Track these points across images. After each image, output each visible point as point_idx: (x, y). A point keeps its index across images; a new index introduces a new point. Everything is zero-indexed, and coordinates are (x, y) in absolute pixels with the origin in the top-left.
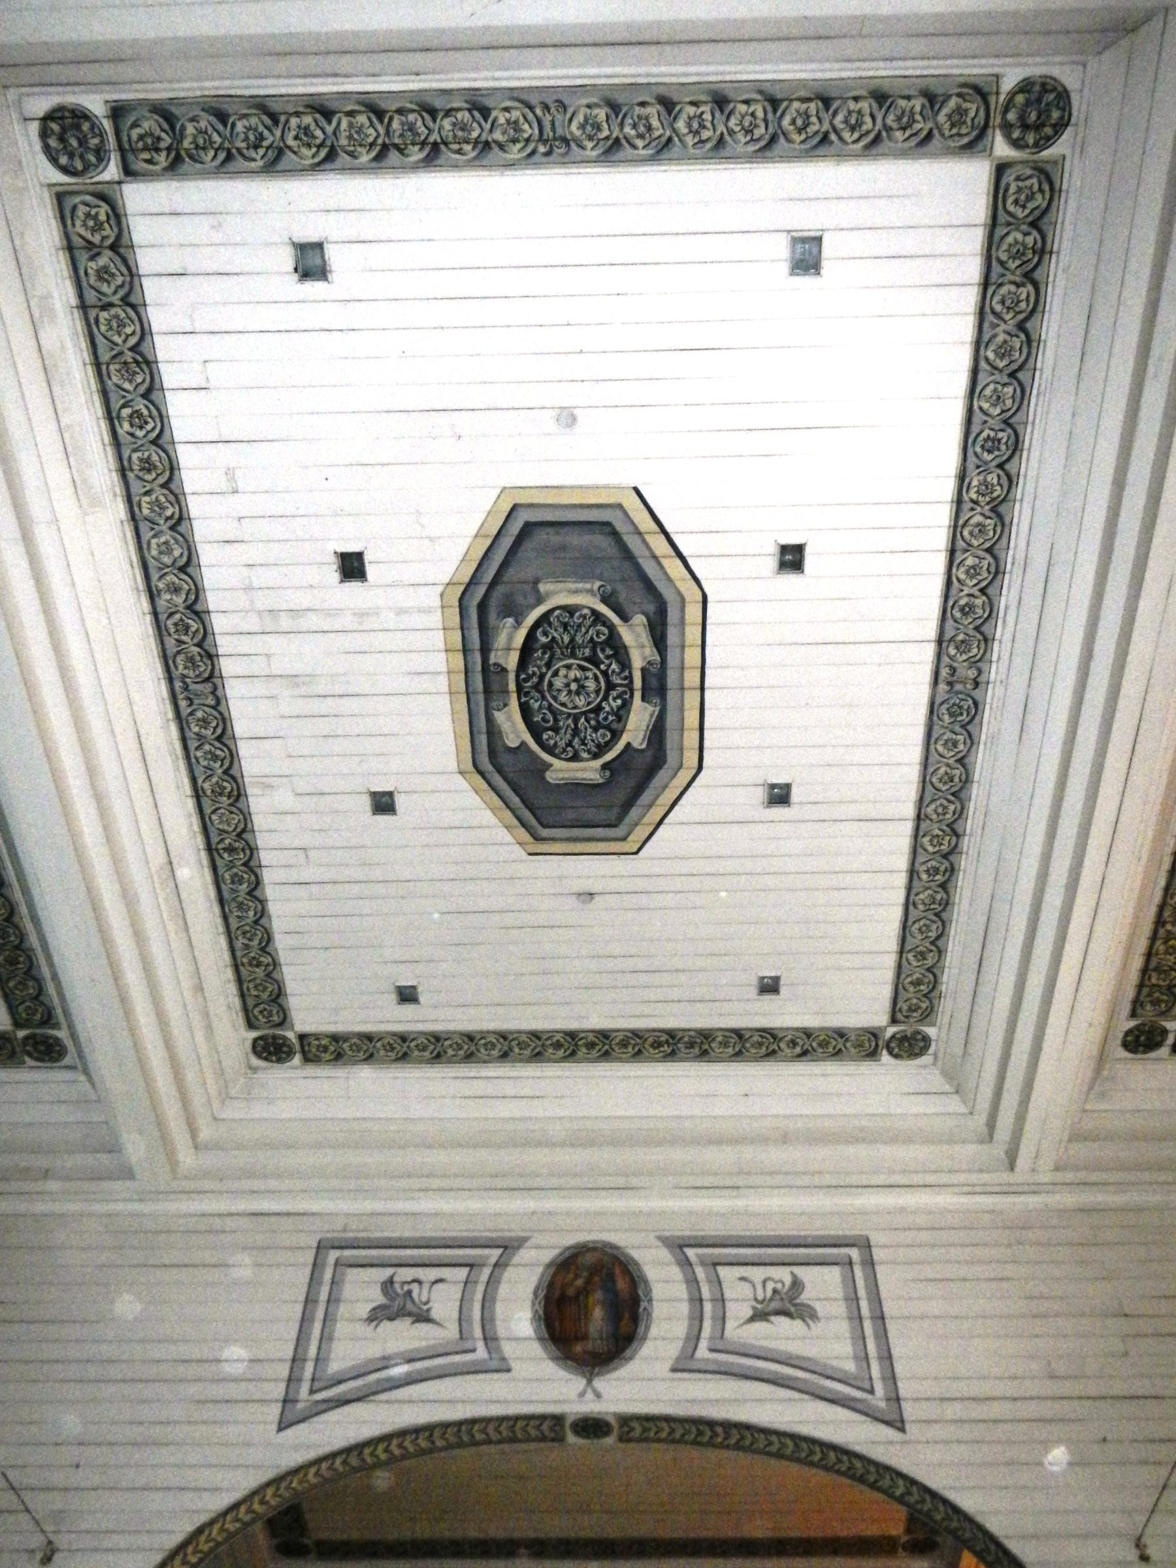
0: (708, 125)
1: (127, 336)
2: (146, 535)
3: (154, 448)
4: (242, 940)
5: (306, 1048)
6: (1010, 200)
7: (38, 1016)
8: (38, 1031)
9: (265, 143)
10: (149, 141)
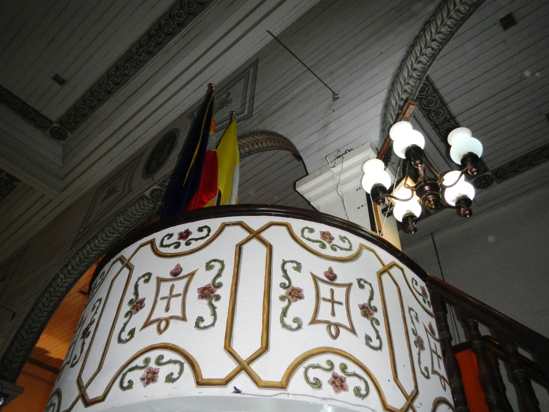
0: (106, 87)
6: (42, 119)
9: (187, 6)
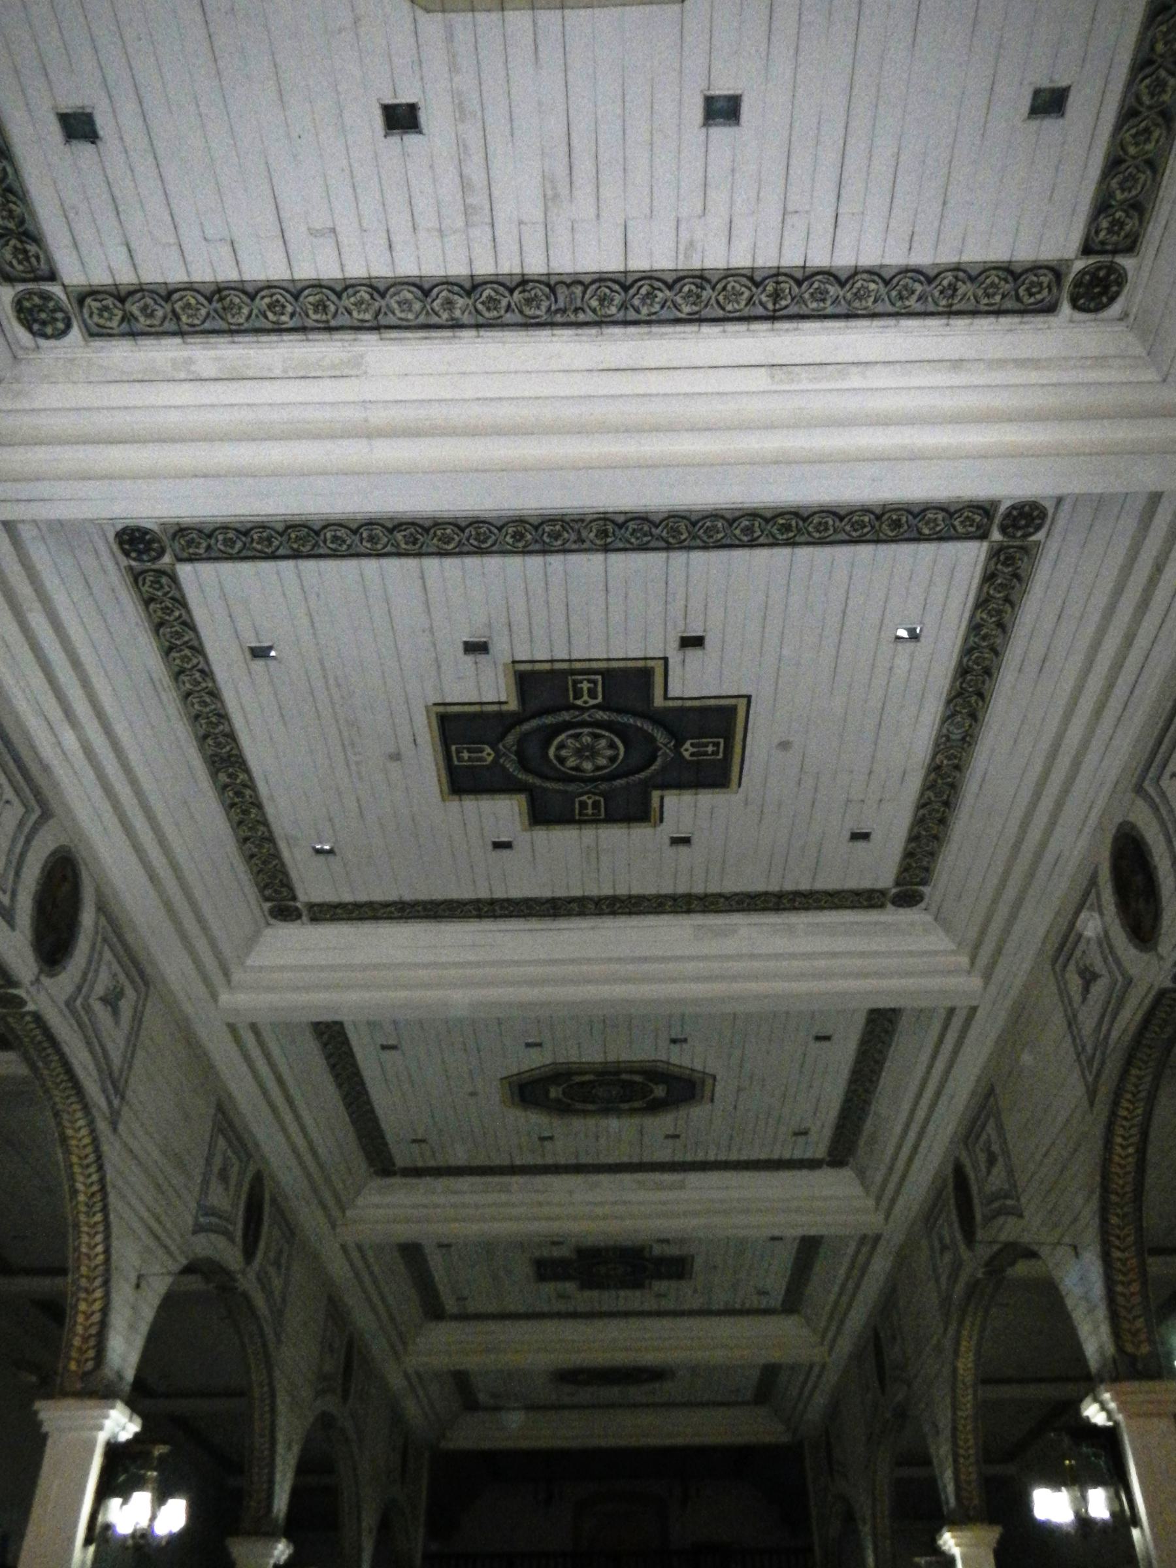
1: (198, 303)
2: (391, 319)
3: (301, 299)
4: (912, 302)
5: (1109, 247)
7: (978, 518)
8: (997, 521)
10: (21, 257)
